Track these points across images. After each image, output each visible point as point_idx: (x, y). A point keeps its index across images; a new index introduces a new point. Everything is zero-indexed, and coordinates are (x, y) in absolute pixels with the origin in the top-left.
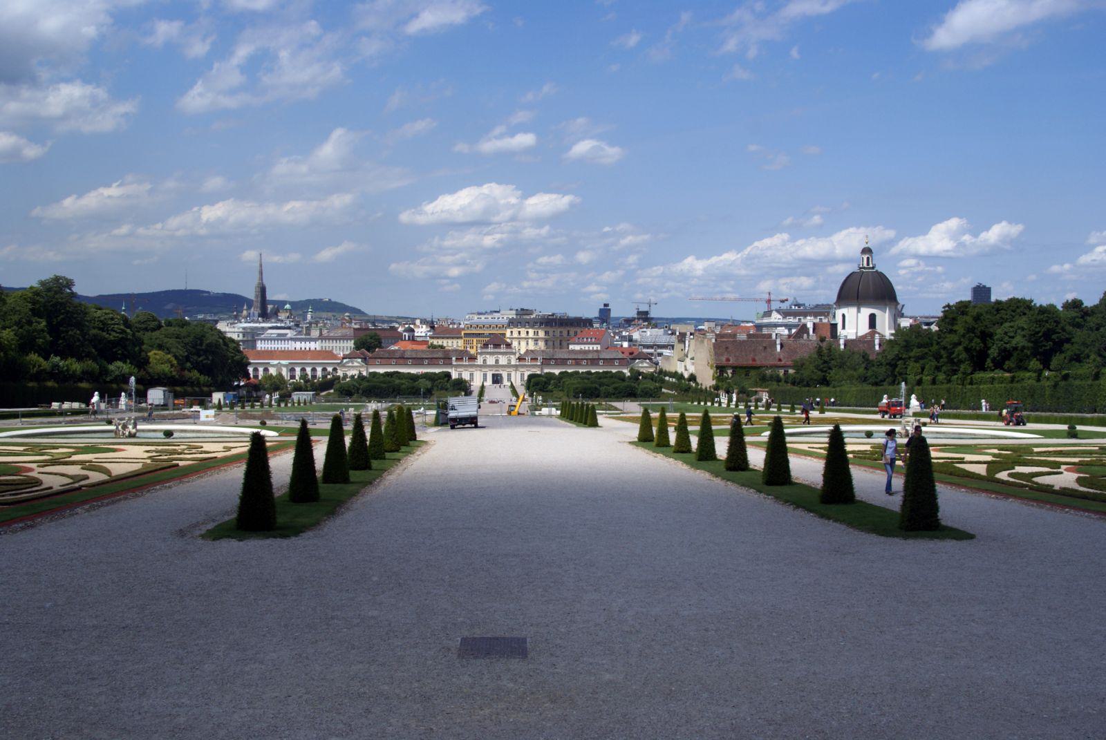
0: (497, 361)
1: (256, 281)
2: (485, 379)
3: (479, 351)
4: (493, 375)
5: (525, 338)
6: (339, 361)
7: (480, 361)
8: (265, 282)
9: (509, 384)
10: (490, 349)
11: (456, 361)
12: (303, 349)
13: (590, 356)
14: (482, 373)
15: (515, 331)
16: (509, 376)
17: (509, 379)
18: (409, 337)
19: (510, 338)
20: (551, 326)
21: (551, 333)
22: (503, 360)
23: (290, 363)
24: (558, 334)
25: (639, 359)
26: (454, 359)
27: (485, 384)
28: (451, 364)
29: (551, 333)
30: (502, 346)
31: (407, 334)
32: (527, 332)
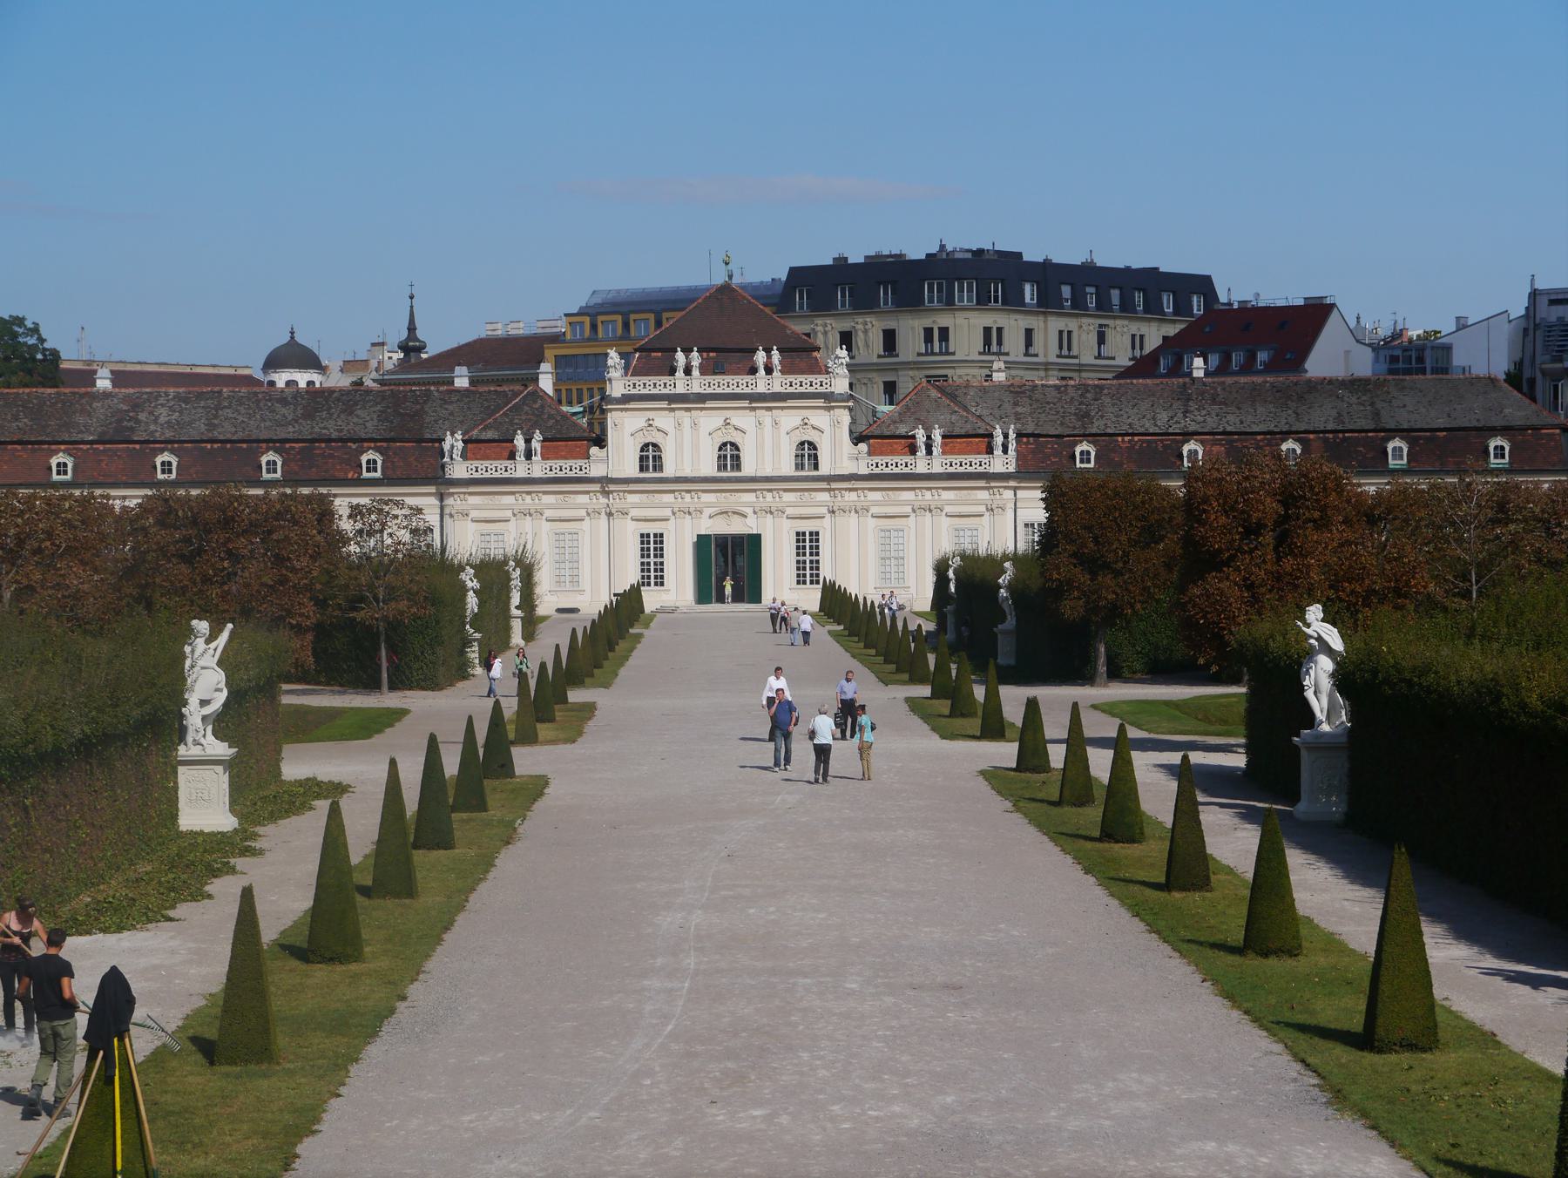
0: (730, 455)
4: (702, 543)
7: (620, 456)
9: (811, 598)
11: (464, 456)
13: (1322, 416)
16: (807, 544)
17: (807, 570)
20: (1013, 301)
21: (1014, 344)
22: (768, 441)
26: (453, 442)
27: (652, 599)
29: (1014, 344)
30: (760, 357)
32: (890, 338)
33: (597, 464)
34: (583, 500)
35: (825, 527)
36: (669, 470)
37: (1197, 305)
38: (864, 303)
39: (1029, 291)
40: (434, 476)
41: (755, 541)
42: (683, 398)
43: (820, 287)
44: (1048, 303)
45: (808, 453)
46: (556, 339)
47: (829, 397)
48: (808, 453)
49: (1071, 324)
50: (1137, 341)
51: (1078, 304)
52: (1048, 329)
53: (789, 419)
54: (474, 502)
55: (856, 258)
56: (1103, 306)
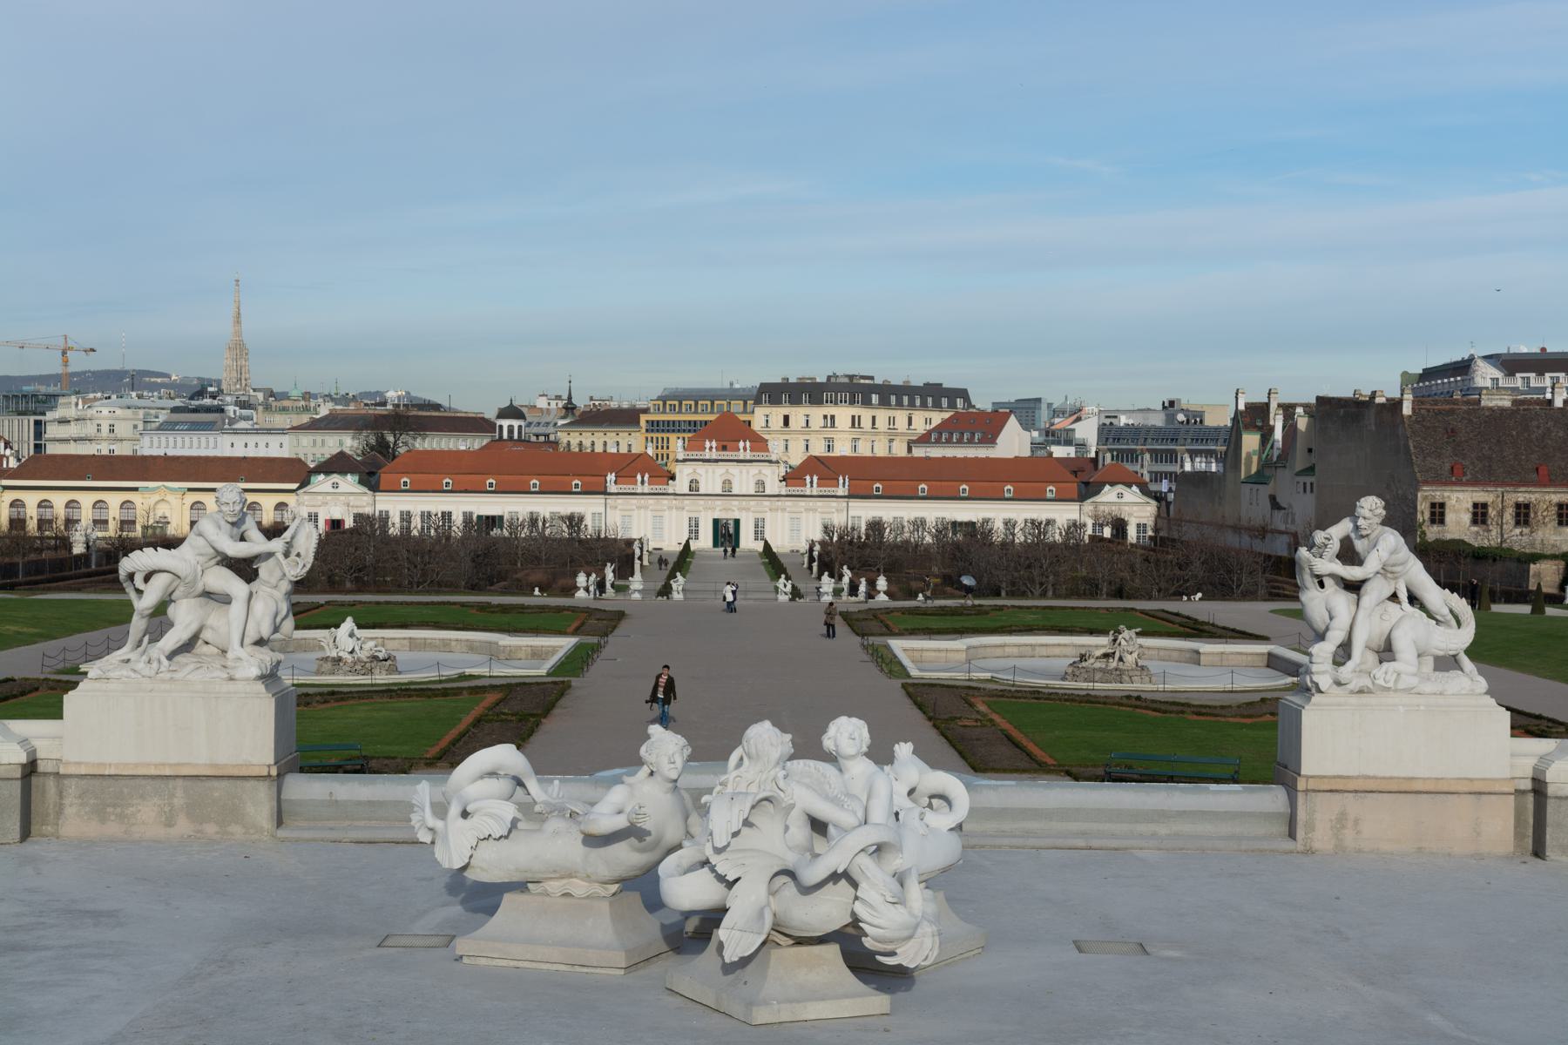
0: (727, 483)
2: (694, 531)
3: (680, 457)
7: (681, 485)
9: (760, 546)
10: (711, 449)
14: (685, 516)
15: (777, 414)
17: (759, 533)
18: (511, 429)
20: (867, 403)
21: (866, 423)
22: (744, 478)
23: (190, 490)
24: (882, 424)
25: (1112, 484)
26: (611, 477)
27: (694, 546)
29: (866, 423)
30: (741, 444)
31: (505, 423)
33: (672, 487)
34: (665, 501)
35: (768, 517)
37: (960, 403)
38: (795, 401)
39: (875, 398)
40: (604, 492)
42: (708, 461)
43: (772, 393)
44: (885, 403)
47: (770, 461)
50: (928, 421)
51: (900, 404)
52: (882, 415)
53: (753, 469)
54: (620, 501)
55: (793, 380)
56: (912, 405)
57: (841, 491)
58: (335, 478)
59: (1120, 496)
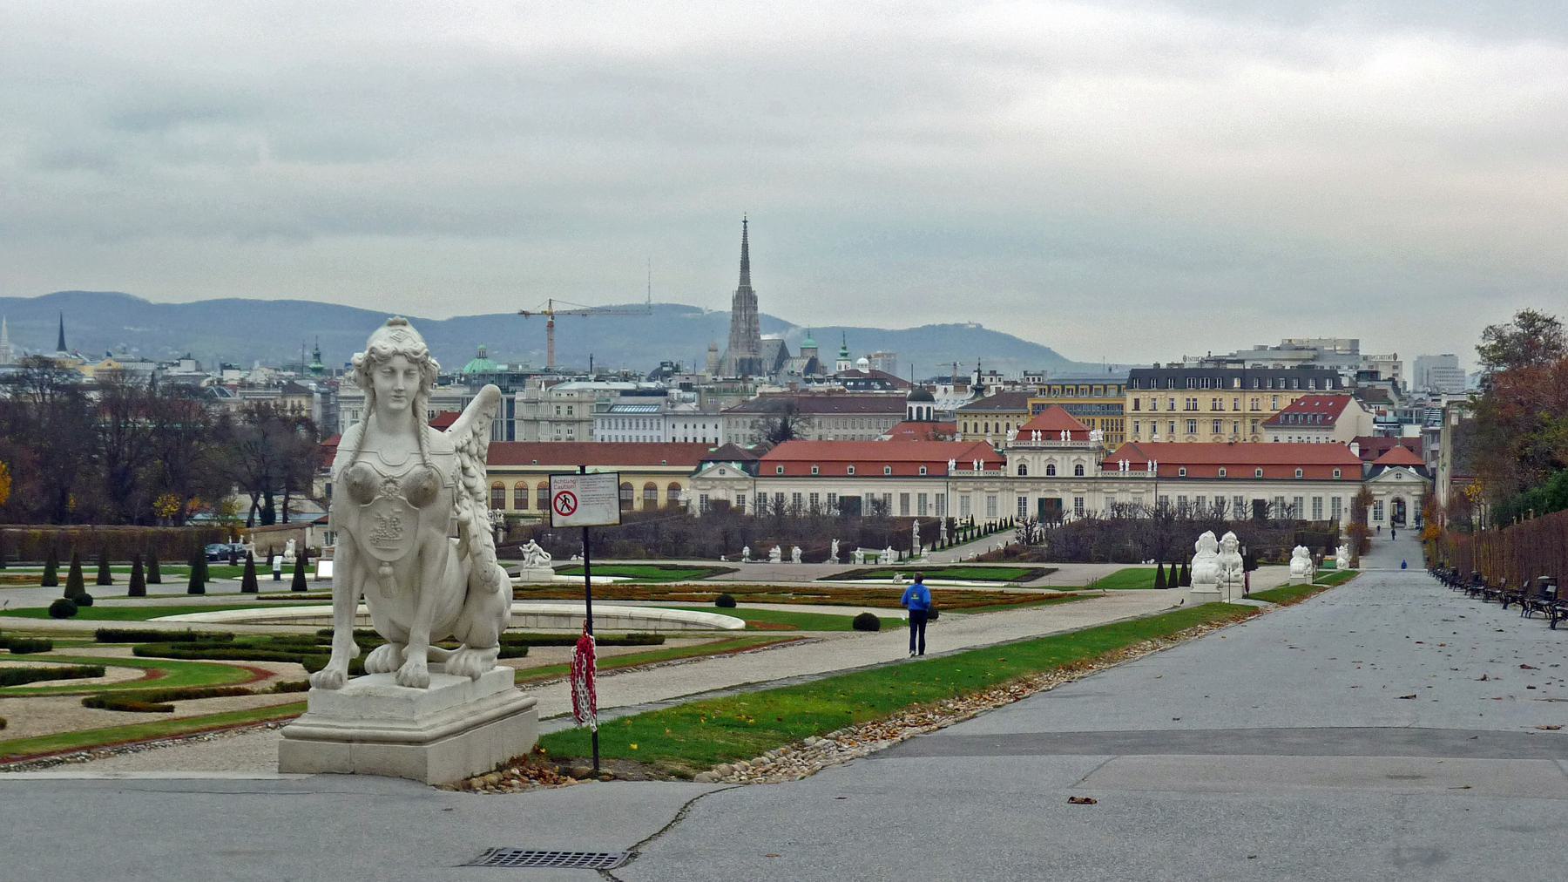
0: (1051, 470)
1: (734, 284)
4: (1041, 501)
5: (1167, 416)
6: (693, 468)
7: (1012, 469)
8: (755, 284)
12: (690, 440)
15: (1145, 397)
17: (1080, 512)
18: (919, 410)
19: (1132, 416)
20: (1227, 386)
25: (1391, 466)
26: (952, 463)
28: (946, 476)
31: (914, 406)
36: (1029, 474)
39: (1237, 383)
41: (1059, 501)
44: (1245, 386)
45: (1079, 470)
46: (1033, 395)
48: (1079, 470)
49: (1259, 396)
52: (1246, 402)
53: (1074, 457)
57: (1150, 473)
58: (723, 465)
59: (1399, 476)
